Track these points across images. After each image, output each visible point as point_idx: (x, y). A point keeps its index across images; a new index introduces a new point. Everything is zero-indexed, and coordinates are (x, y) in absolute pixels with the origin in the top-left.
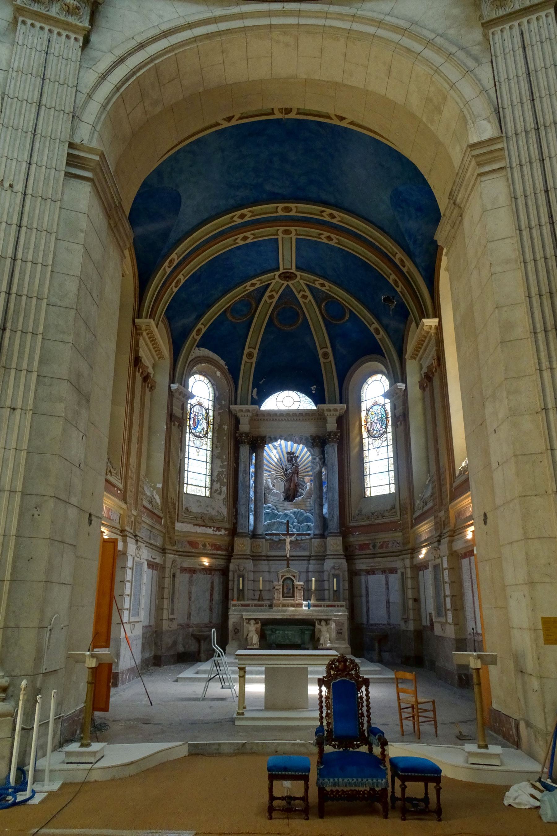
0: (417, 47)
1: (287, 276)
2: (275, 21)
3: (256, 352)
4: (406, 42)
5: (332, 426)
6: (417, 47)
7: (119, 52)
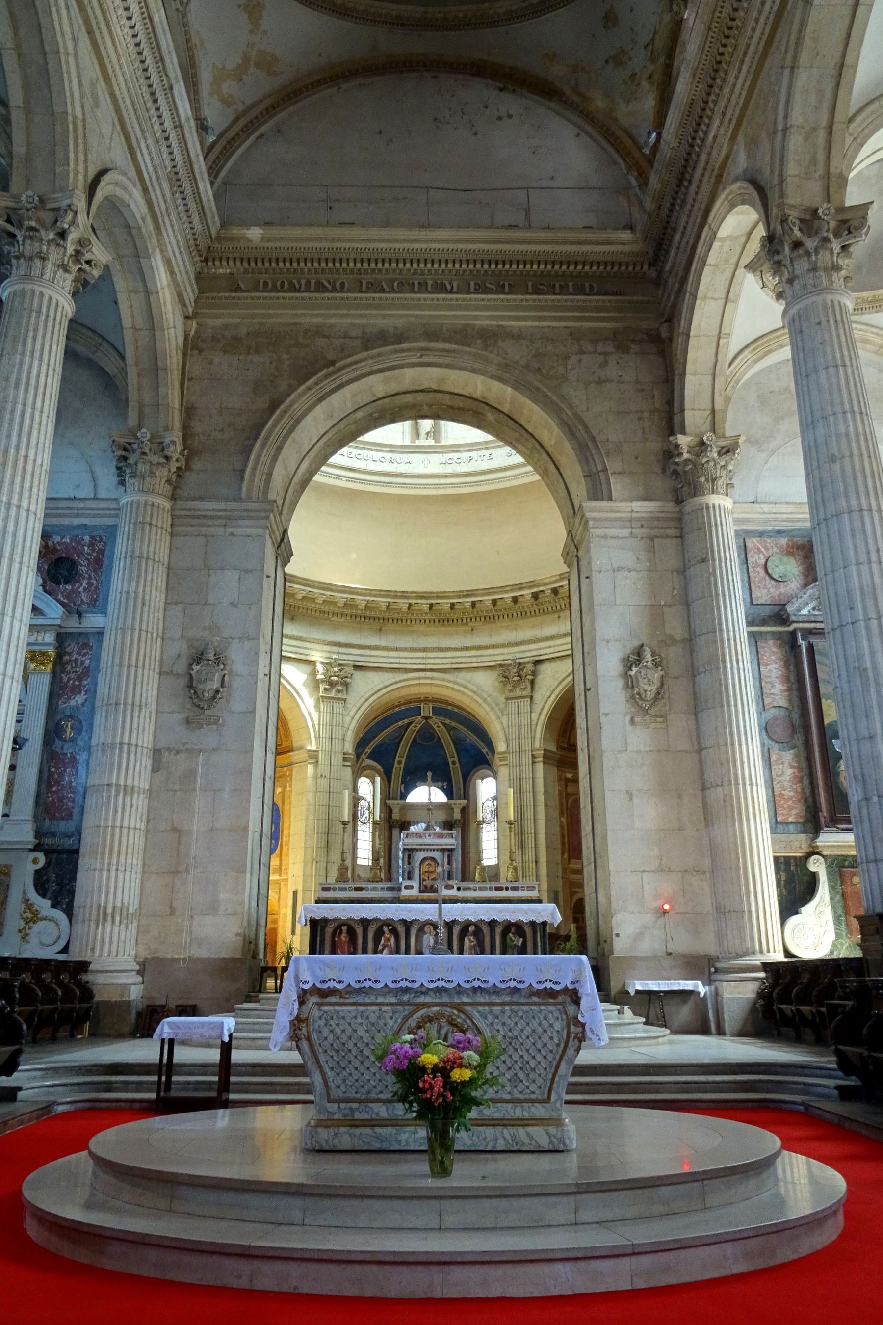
0: (480, 701)
1: (426, 718)
2: (422, 681)
3: (403, 760)
4: (476, 697)
5: (457, 815)
6: (480, 701)
7: (358, 705)
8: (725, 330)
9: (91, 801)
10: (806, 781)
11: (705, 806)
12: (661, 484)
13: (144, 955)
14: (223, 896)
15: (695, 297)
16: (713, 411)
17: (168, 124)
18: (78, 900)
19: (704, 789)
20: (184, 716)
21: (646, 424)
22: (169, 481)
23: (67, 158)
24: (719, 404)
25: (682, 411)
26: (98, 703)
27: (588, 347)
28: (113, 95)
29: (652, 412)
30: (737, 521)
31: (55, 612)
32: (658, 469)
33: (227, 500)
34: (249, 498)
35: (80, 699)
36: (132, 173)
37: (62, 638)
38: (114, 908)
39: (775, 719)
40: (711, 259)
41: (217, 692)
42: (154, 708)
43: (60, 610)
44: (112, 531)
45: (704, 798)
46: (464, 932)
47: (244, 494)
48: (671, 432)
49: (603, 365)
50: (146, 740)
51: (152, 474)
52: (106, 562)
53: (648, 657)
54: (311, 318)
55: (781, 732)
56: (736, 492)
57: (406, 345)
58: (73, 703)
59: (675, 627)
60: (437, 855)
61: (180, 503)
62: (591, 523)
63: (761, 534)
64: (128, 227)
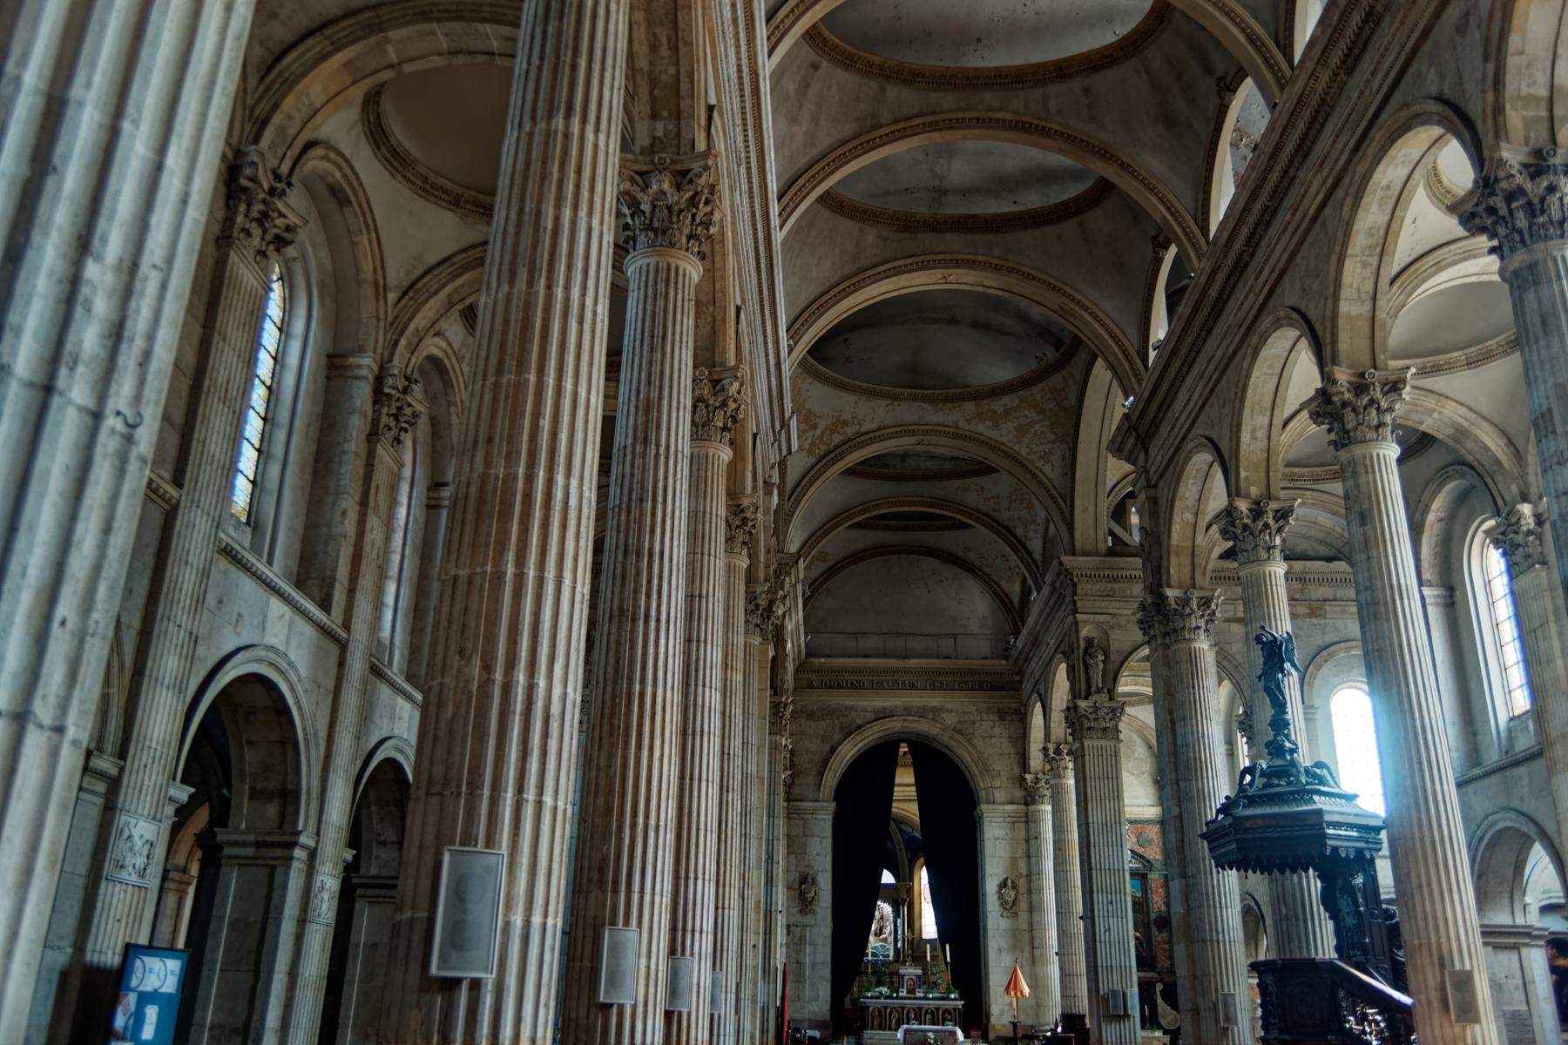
12: (1019, 794)
14: (820, 993)
27: (985, 716)
29: (1017, 754)
46: (926, 1012)
49: (992, 728)
53: (1010, 884)
54: (848, 702)
59: (1023, 868)
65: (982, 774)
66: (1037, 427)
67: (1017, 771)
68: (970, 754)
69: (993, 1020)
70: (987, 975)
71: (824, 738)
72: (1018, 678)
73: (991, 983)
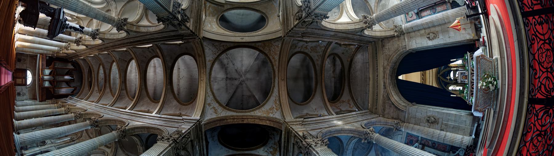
8: (379, 31)
9: (445, 142)
10: (440, 5)
11: (448, 23)
12: (402, 37)
13: (469, 135)
15: (376, 36)
16: (391, 30)
17: (356, 115)
18: (458, 146)
19: (446, 23)
20: (436, 125)
21: (394, 41)
22: (402, 123)
23: (360, 130)
24: (389, 29)
25: (391, 35)
26: (431, 139)
28: (353, 122)
30: (405, 24)
31: (417, 144)
32: (400, 38)
33: (406, 113)
34: (406, 110)
35: (430, 142)
36: (362, 122)
37: (420, 144)
38: (461, 140)
39: (432, 12)
40: (371, 35)
41: (434, 118)
42: (434, 130)
43: (417, 143)
44: (408, 133)
45: (447, 23)
47: (405, 110)
48: (395, 36)
50: (439, 131)
51: (400, 125)
52: (411, 135)
55: (434, 10)
56: (401, 24)
57: (386, 82)
58: (430, 143)
60: (462, 76)
61: (405, 121)
62: (410, 48)
63: (406, 19)
64: (368, 123)
65: (399, 51)
66: (273, 50)
67: (396, 39)
68: (394, 56)
69: (472, 38)
70: (459, 42)
71: (390, 107)
72: (373, 43)
73: (460, 40)
